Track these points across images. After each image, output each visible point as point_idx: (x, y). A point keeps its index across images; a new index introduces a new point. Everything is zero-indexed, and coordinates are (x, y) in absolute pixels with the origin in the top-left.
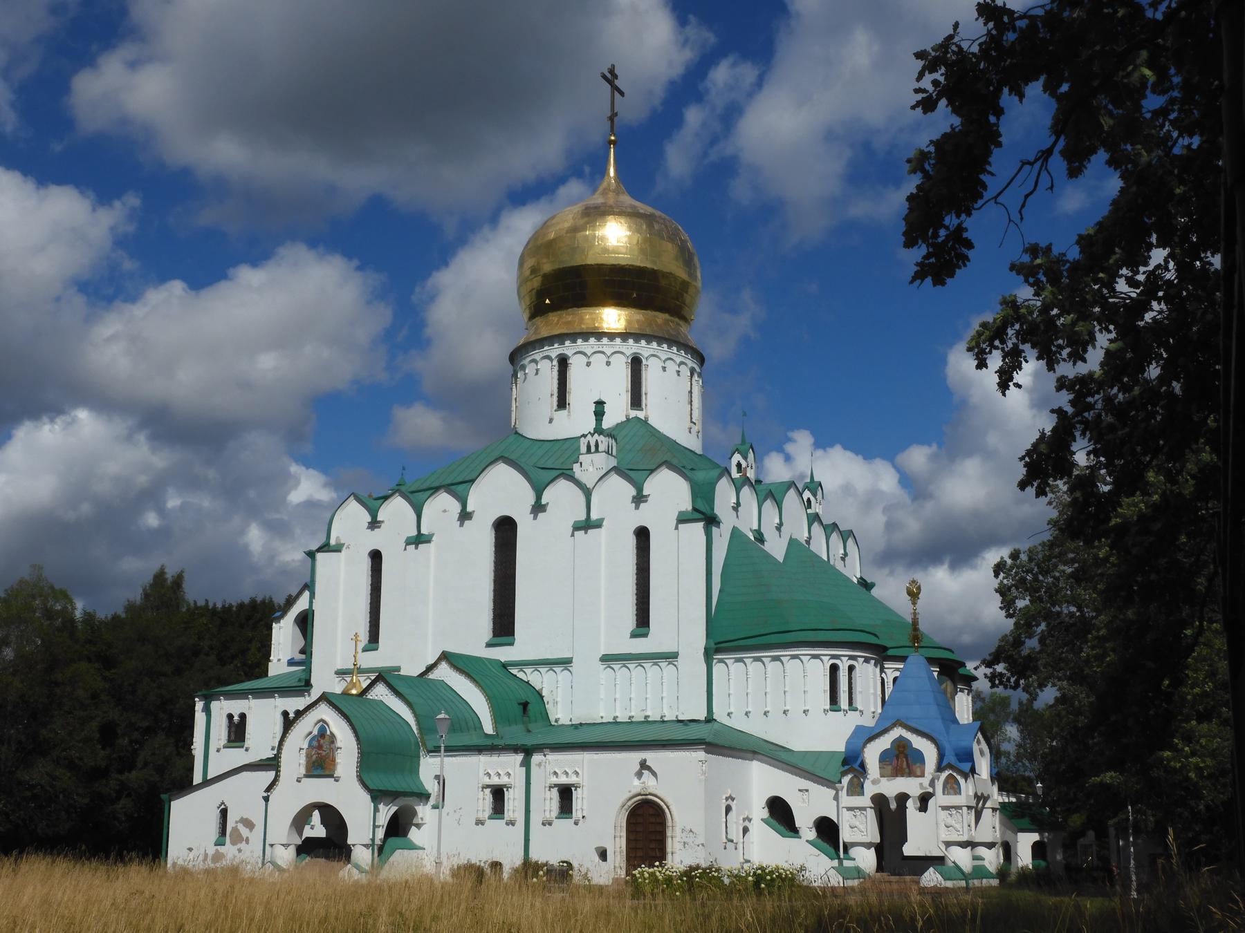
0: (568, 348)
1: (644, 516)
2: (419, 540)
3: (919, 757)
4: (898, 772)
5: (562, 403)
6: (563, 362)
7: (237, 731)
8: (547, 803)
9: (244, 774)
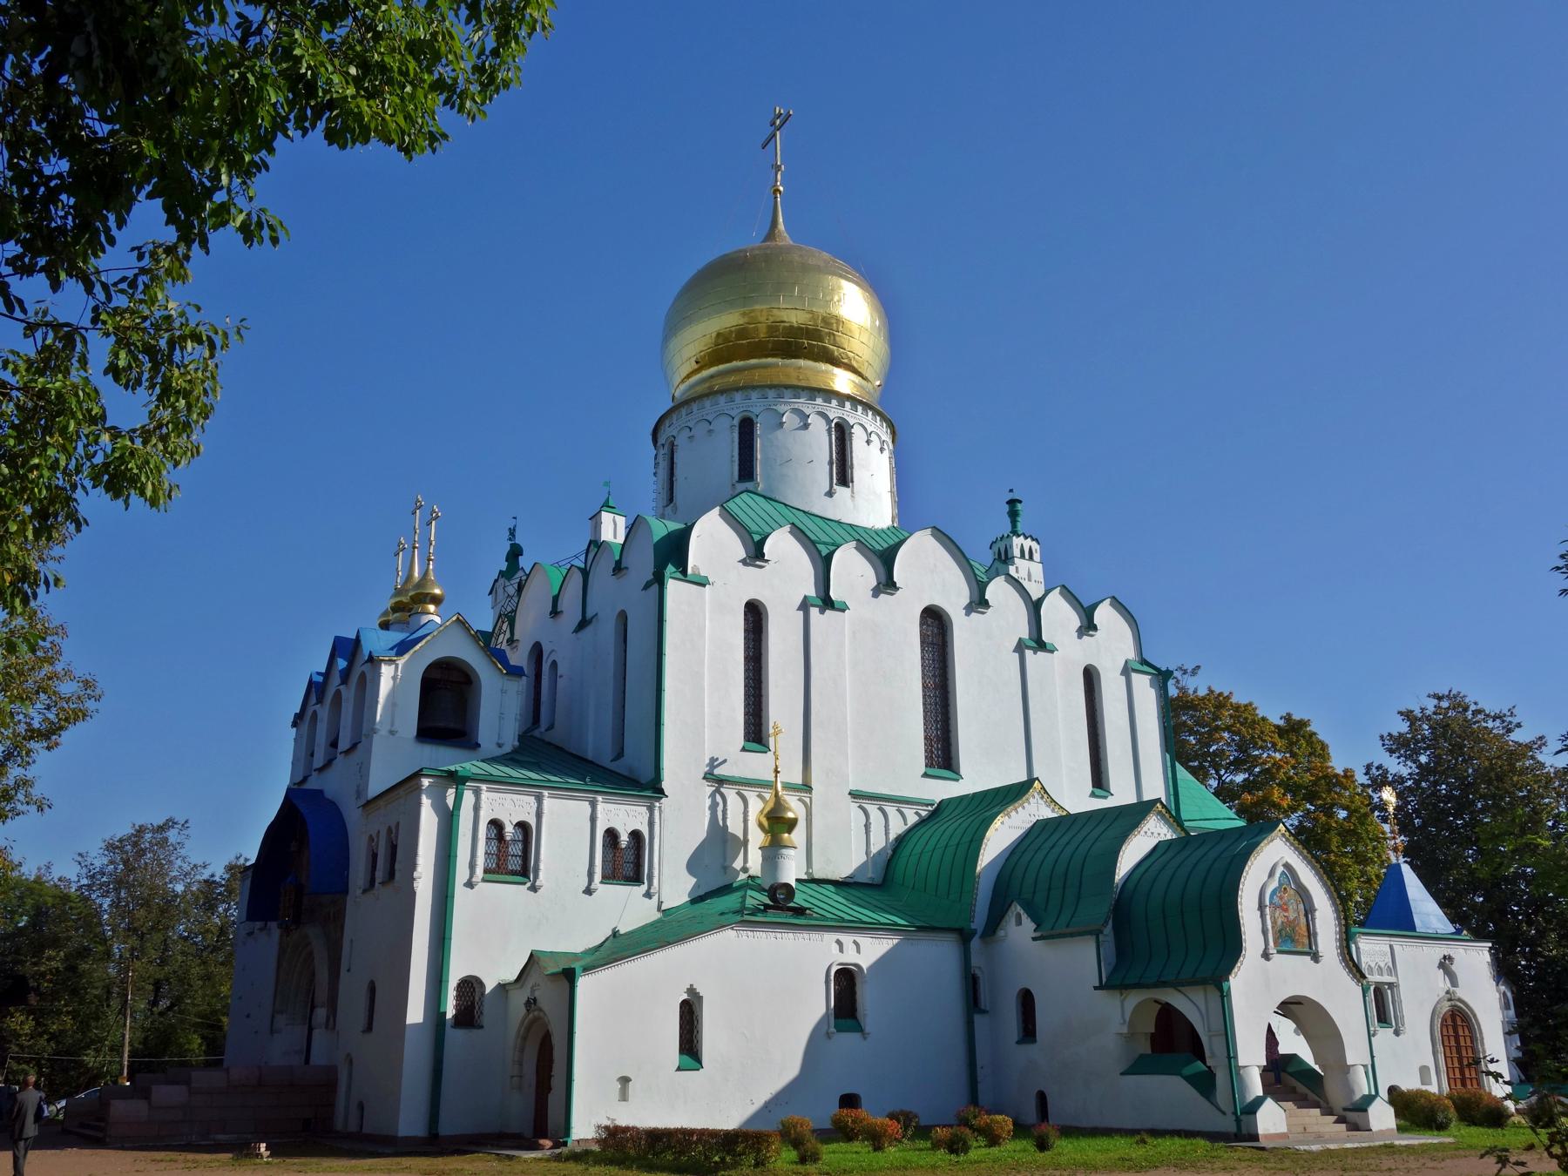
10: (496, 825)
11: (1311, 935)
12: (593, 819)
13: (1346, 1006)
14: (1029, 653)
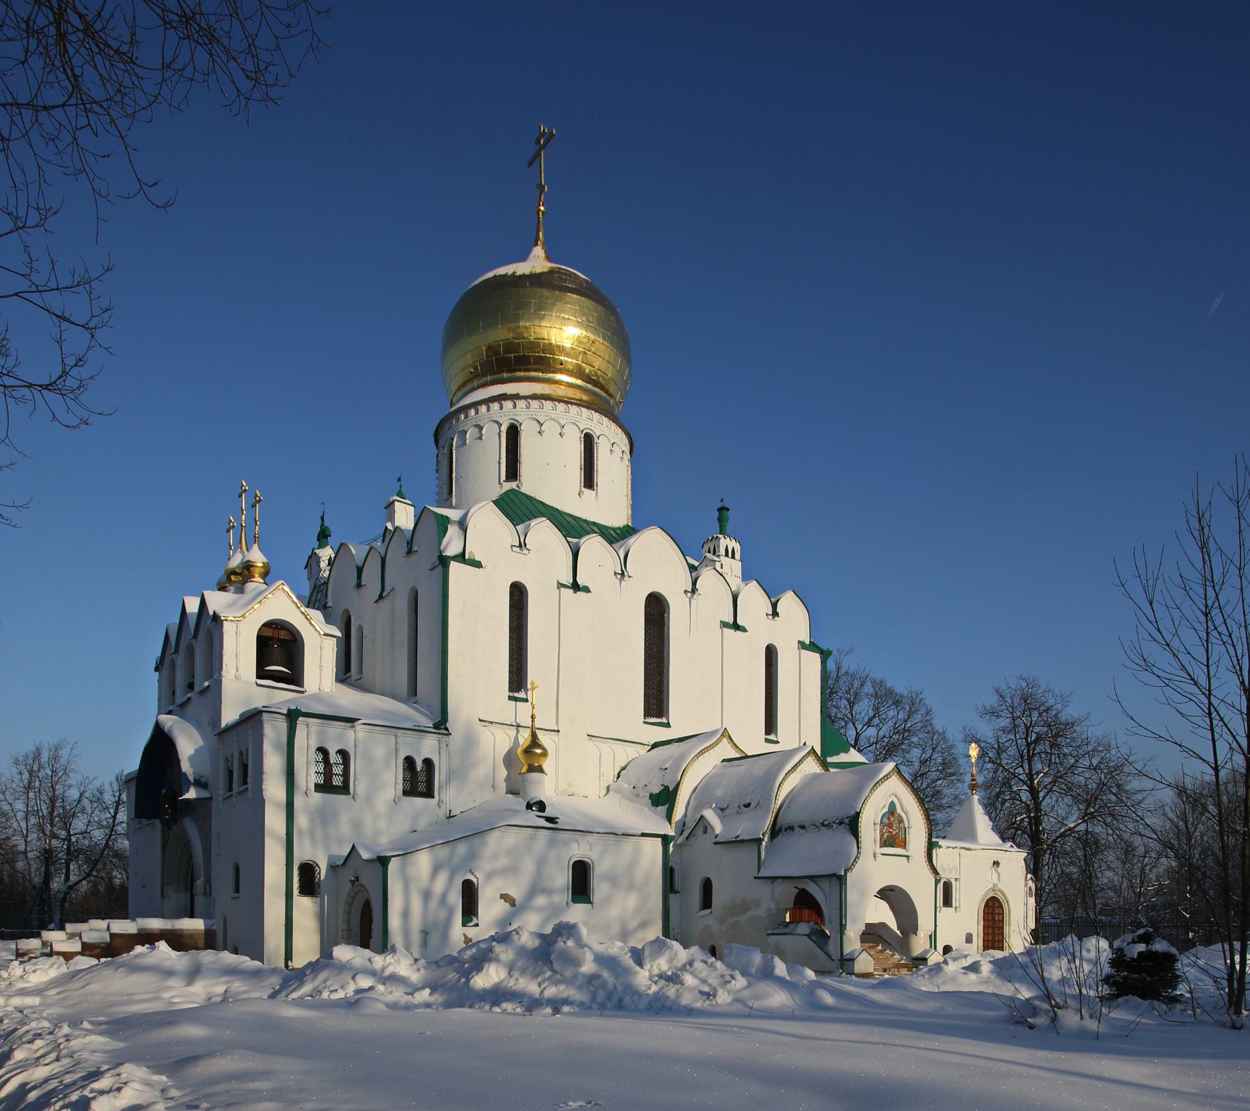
10: (322, 751)
13: (923, 896)
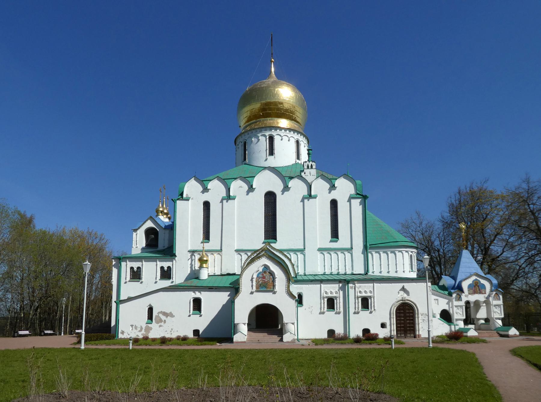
0: (273, 133)
1: (334, 195)
2: (229, 197)
3: (484, 286)
4: (475, 292)
5: (272, 153)
6: (271, 139)
7: (136, 275)
8: (354, 304)
9: (161, 294)
11: (274, 286)
12: (157, 265)
14: (306, 201)
